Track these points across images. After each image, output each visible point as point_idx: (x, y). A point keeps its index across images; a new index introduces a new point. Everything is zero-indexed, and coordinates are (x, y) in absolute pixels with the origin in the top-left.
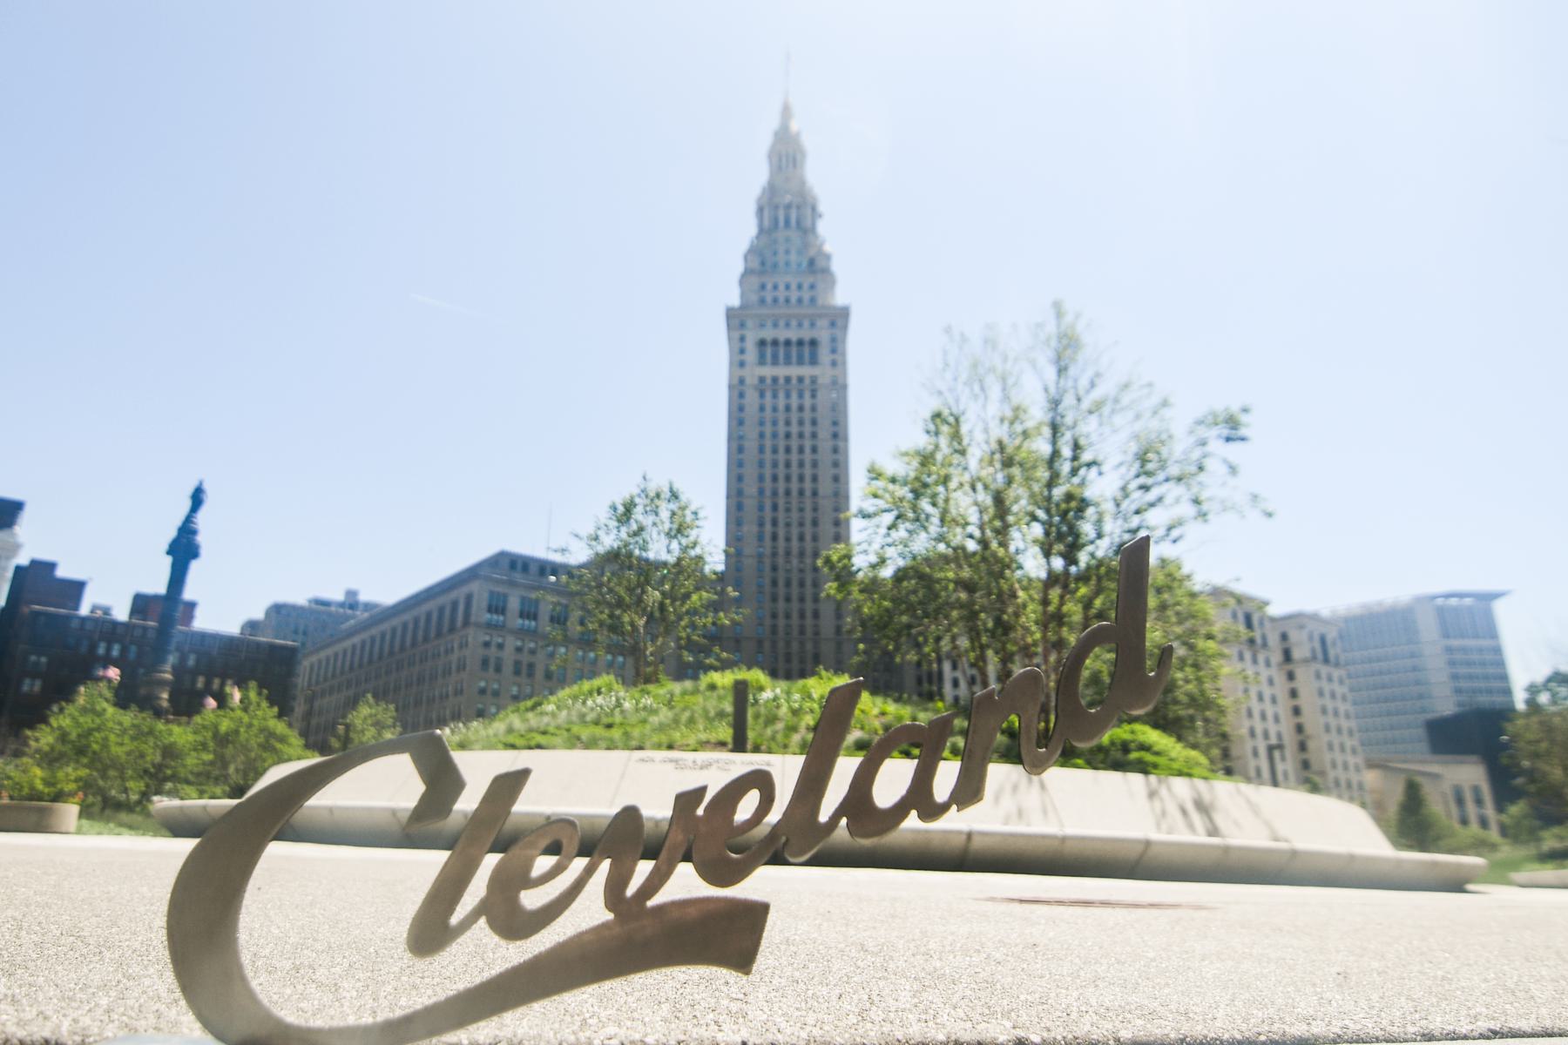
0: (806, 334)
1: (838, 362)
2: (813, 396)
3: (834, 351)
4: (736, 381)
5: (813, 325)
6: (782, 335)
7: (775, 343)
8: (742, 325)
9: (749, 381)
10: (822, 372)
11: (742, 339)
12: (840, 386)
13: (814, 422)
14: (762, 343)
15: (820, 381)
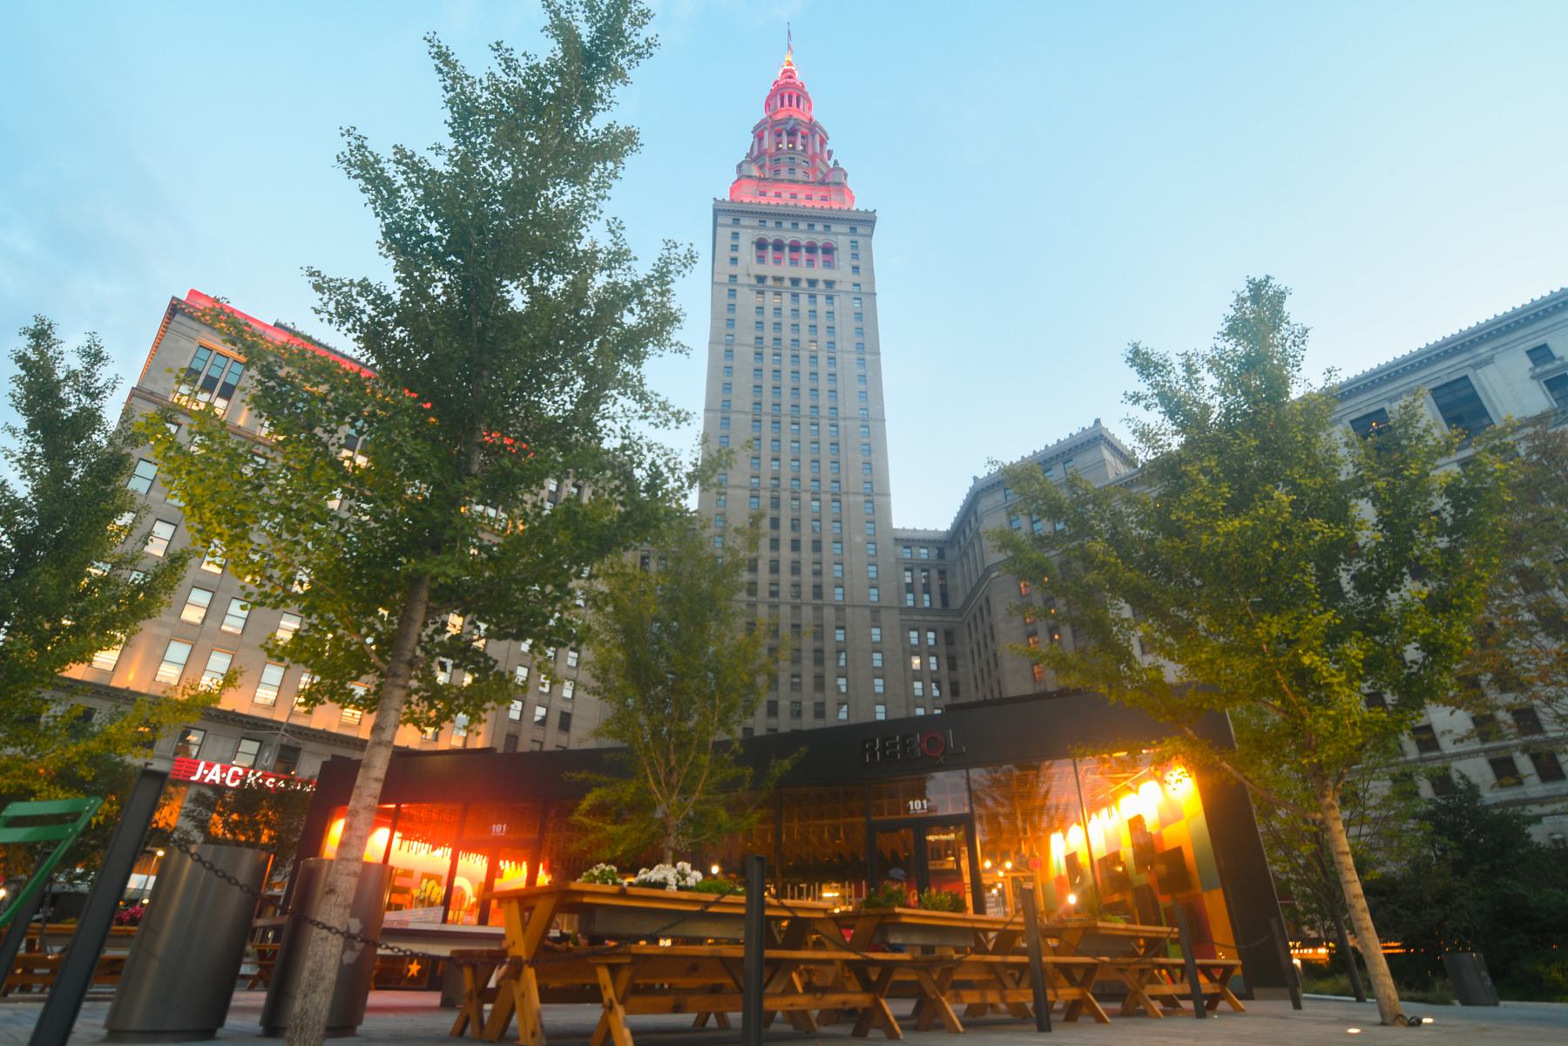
0: (820, 240)
1: (861, 265)
2: (830, 298)
3: (855, 256)
4: (726, 279)
5: (827, 227)
6: (788, 238)
7: (778, 246)
8: (736, 220)
9: (740, 280)
10: (842, 272)
11: (735, 235)
12: (865, 295)
13: (831, 329)
14: (761, 245)
15: (837, 287)
